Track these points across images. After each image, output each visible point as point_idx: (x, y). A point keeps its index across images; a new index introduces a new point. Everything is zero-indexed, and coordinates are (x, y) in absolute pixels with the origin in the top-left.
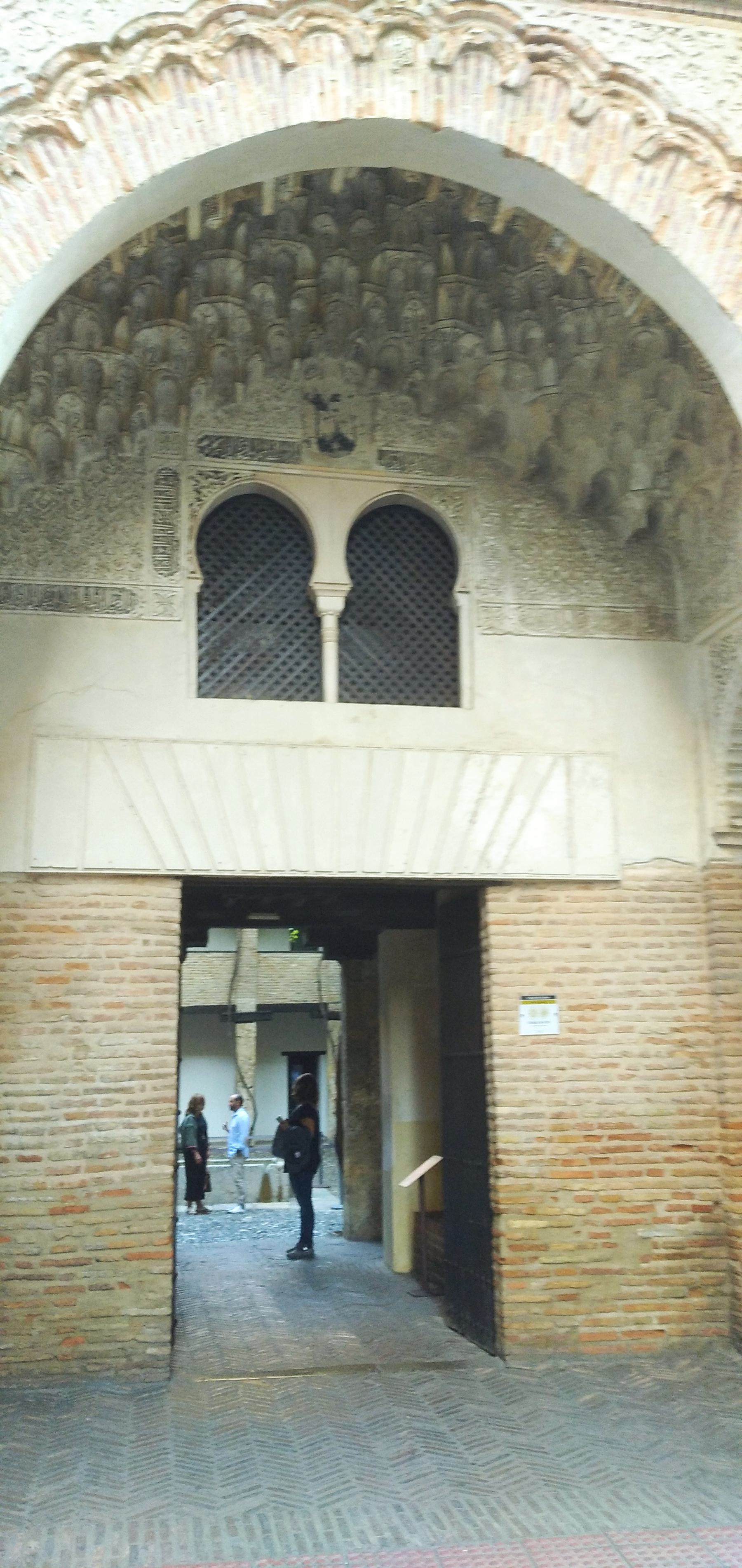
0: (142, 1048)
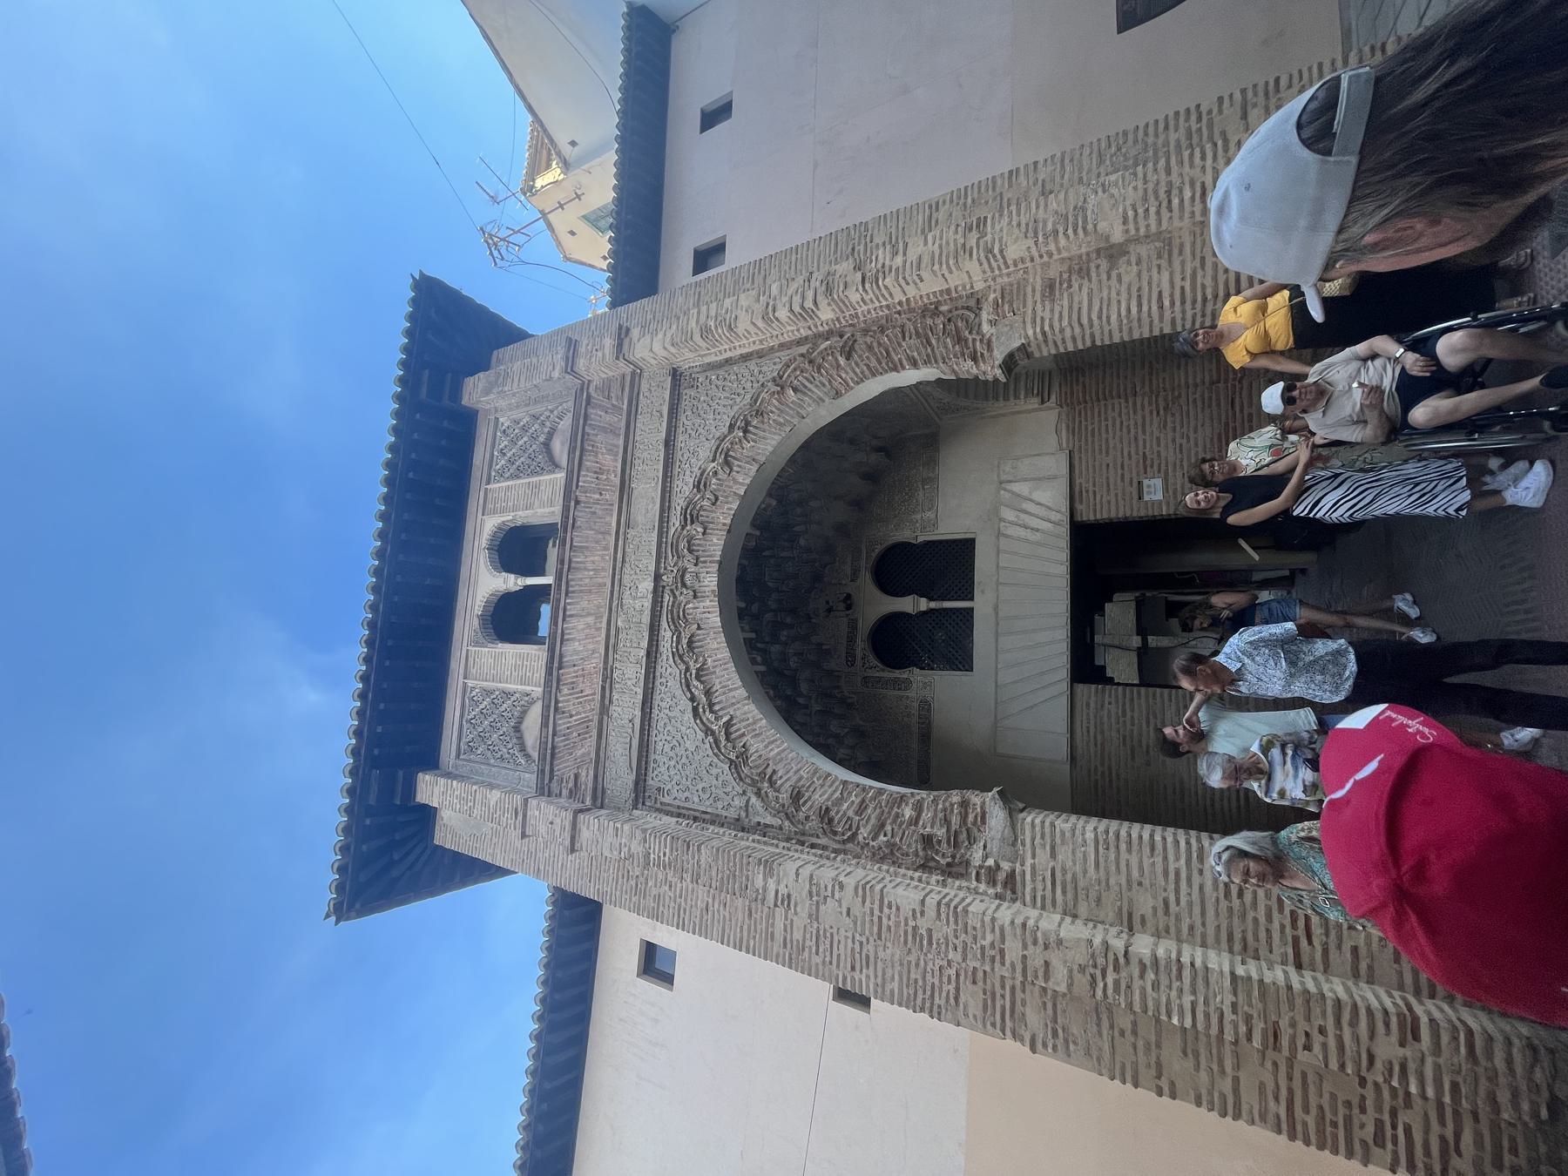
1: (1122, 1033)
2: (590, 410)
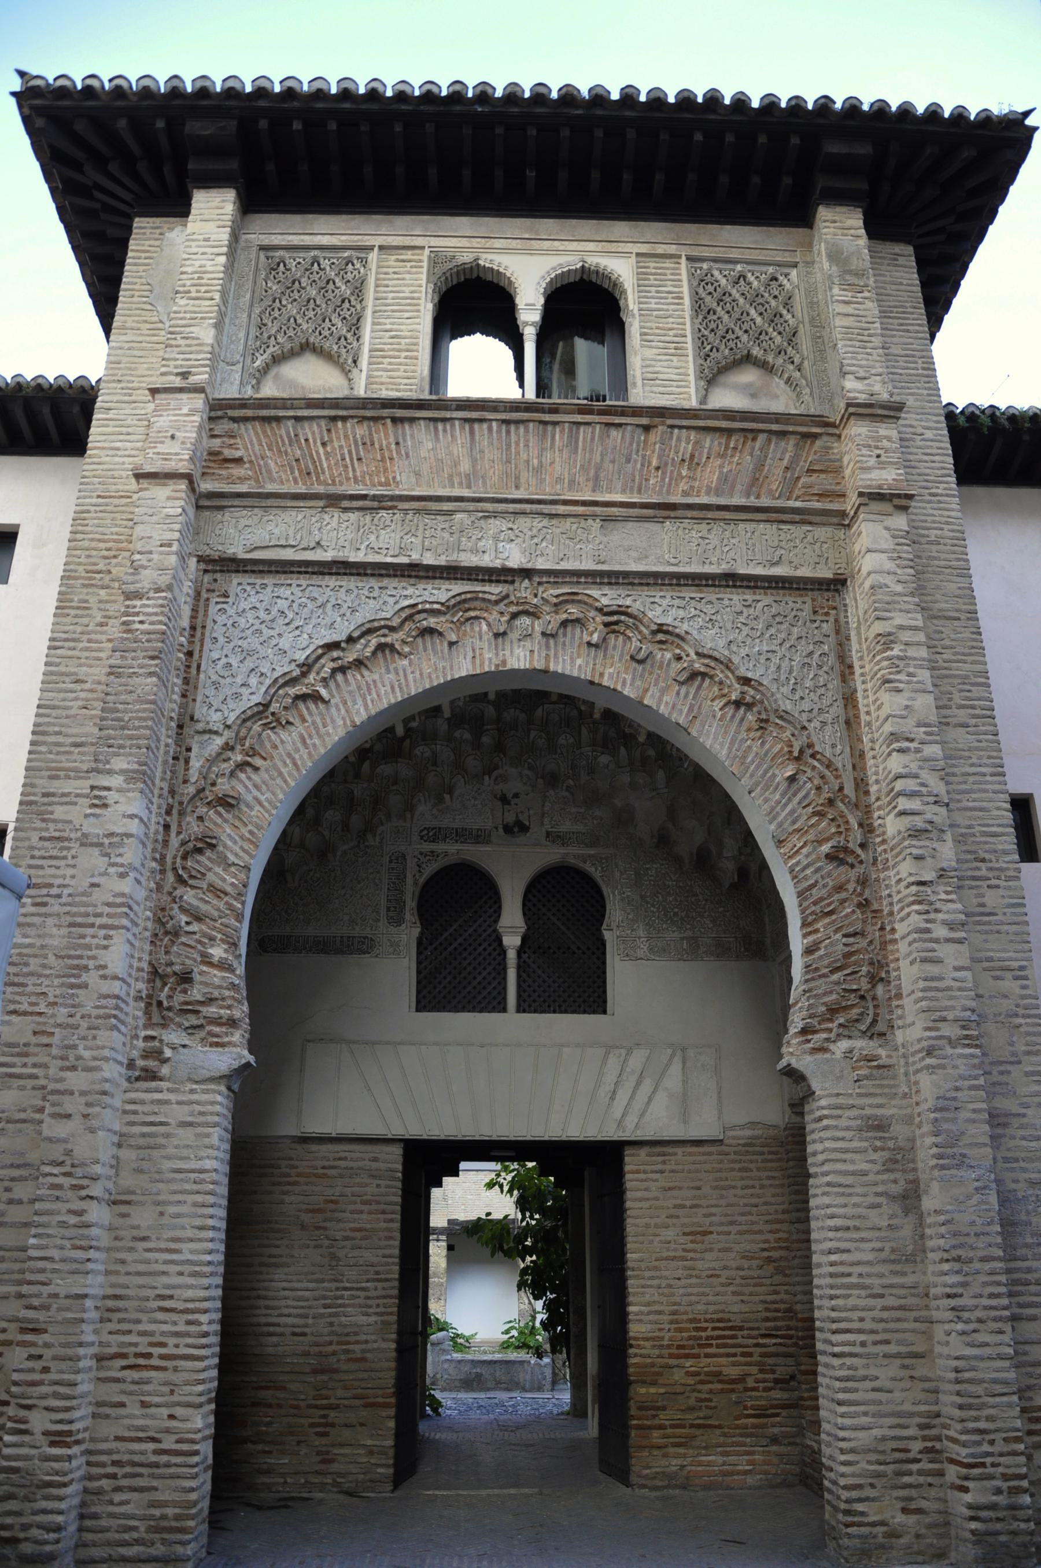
0: (375, 1260)
1: (8, 1190)
2: (792, 441)
